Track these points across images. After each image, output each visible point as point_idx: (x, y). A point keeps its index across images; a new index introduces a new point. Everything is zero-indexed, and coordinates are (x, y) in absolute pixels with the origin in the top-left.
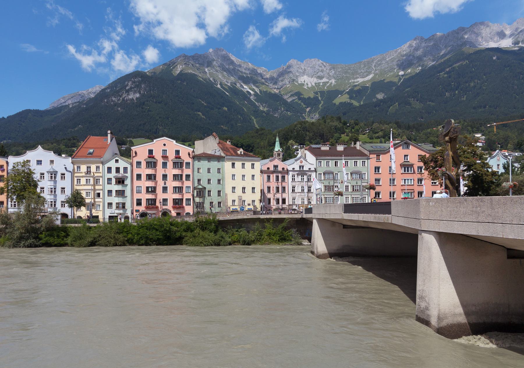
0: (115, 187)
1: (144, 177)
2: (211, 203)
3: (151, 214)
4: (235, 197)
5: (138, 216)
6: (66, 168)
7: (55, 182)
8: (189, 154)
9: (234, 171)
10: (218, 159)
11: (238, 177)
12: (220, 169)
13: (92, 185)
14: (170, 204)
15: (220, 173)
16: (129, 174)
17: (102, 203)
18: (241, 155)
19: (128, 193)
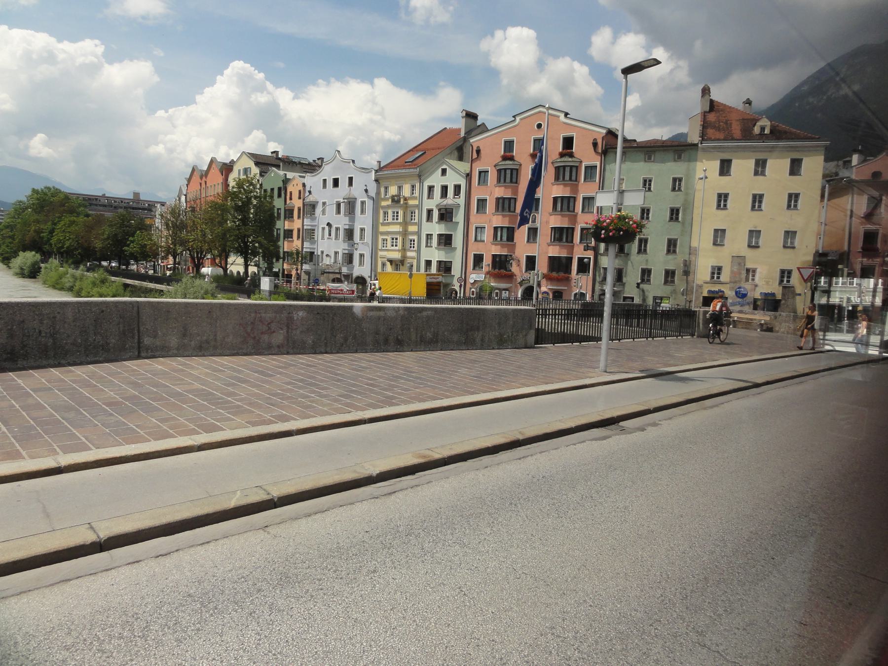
0: (437, 228)
1: (490, 206)
2: (646, 274)
3: (499, 289)
4: (723, 257)
5: (473, 292)
6: (366, 191)
7: (352, 220)
8: (595, 145)
9: (724, 184)
10: (675, 151)
11: (739, 203)
12: (680, 180)
13: (400, 224)
14: (542, 266)
15: (679, 189)
16: (461, 200)
17: (416, 260)
18: (762, 136)
19: (458, 240)
